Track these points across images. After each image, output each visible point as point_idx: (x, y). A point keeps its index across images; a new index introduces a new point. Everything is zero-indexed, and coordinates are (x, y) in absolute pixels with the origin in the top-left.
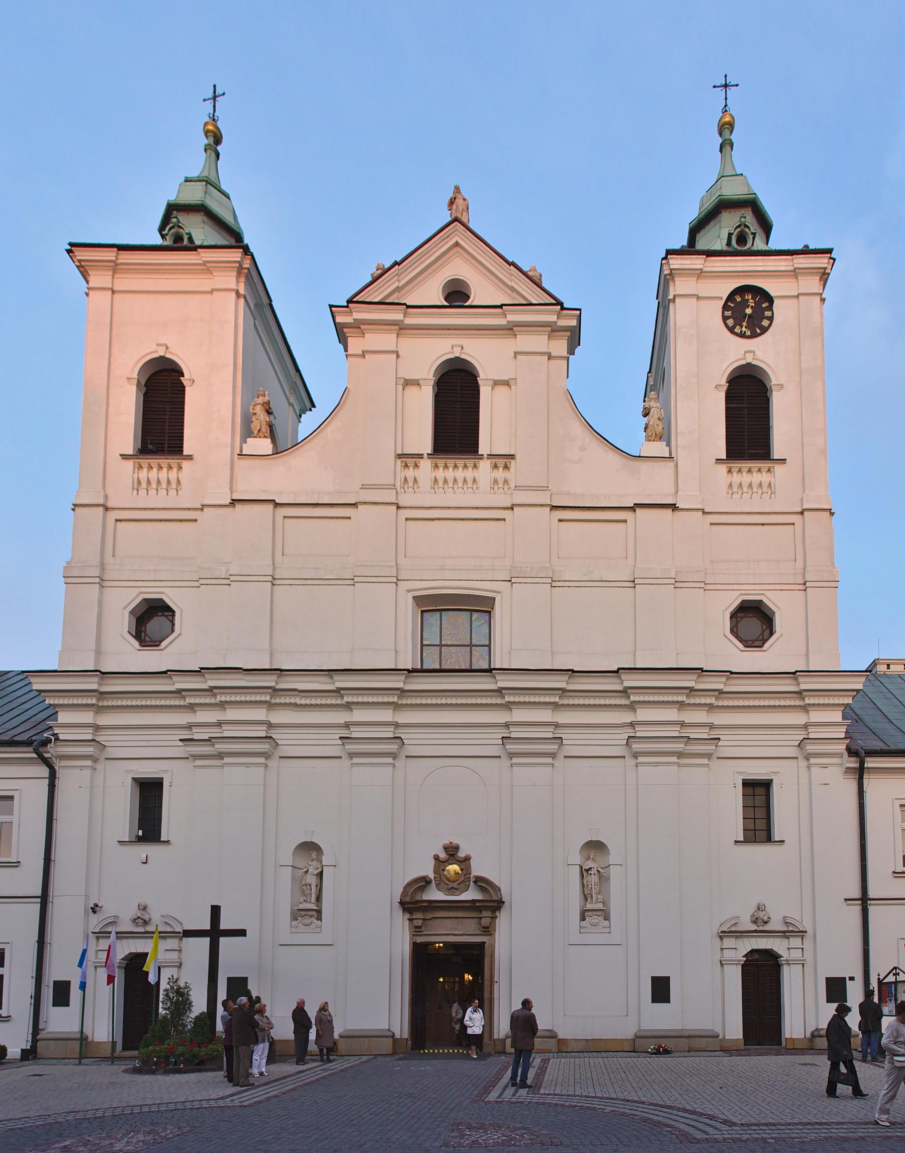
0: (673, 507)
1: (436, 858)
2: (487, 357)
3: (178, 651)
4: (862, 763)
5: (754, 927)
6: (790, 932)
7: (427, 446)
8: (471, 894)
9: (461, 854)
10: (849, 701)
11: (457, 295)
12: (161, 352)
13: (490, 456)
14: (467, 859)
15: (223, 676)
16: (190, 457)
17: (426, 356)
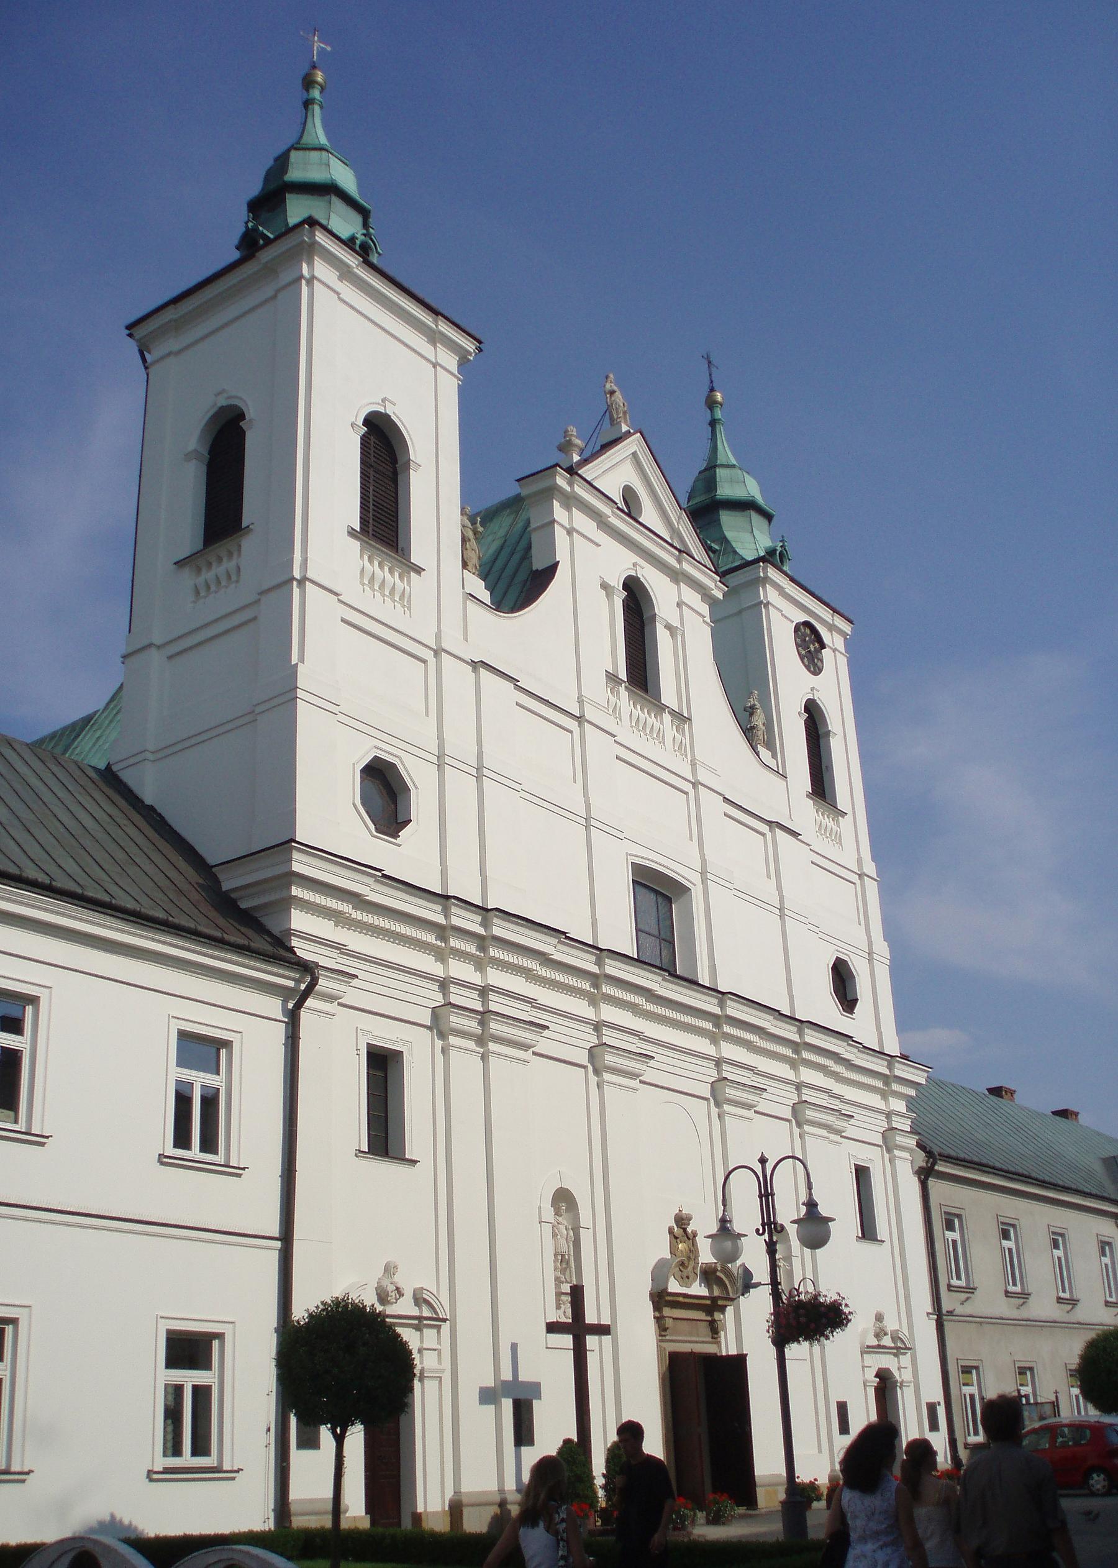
0: (795, 834)
1: (671, 1231)
2: (664, 595)
3: (411, 855)
4: (934, 1164)
5: (875, 1342)
6: (900, 1348)
7: (623, 675)
8: (698, 1289)
9: (689, 1230)
10: (912, 1092)
11: (630, 505)
12: (222, 402)
13: (673, 713)
14: (695, 1234)
15: (472, 912)
16: (419, 570)
17: (619, 563)
